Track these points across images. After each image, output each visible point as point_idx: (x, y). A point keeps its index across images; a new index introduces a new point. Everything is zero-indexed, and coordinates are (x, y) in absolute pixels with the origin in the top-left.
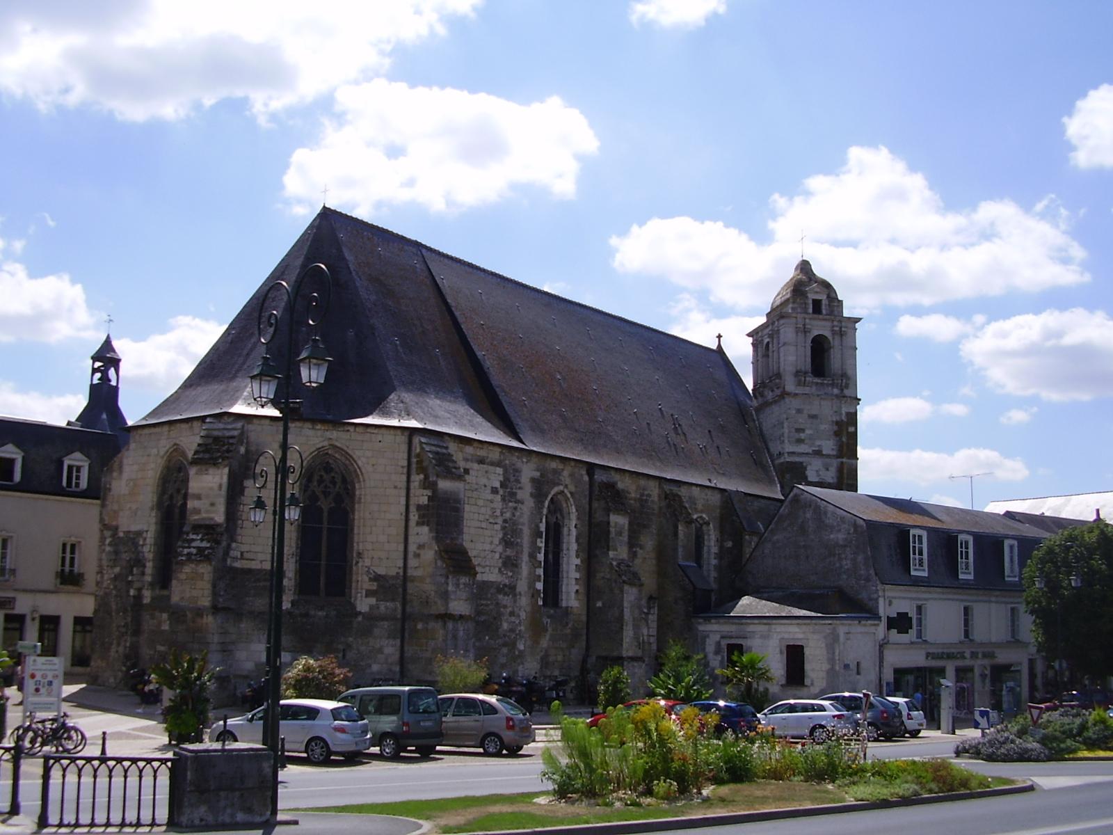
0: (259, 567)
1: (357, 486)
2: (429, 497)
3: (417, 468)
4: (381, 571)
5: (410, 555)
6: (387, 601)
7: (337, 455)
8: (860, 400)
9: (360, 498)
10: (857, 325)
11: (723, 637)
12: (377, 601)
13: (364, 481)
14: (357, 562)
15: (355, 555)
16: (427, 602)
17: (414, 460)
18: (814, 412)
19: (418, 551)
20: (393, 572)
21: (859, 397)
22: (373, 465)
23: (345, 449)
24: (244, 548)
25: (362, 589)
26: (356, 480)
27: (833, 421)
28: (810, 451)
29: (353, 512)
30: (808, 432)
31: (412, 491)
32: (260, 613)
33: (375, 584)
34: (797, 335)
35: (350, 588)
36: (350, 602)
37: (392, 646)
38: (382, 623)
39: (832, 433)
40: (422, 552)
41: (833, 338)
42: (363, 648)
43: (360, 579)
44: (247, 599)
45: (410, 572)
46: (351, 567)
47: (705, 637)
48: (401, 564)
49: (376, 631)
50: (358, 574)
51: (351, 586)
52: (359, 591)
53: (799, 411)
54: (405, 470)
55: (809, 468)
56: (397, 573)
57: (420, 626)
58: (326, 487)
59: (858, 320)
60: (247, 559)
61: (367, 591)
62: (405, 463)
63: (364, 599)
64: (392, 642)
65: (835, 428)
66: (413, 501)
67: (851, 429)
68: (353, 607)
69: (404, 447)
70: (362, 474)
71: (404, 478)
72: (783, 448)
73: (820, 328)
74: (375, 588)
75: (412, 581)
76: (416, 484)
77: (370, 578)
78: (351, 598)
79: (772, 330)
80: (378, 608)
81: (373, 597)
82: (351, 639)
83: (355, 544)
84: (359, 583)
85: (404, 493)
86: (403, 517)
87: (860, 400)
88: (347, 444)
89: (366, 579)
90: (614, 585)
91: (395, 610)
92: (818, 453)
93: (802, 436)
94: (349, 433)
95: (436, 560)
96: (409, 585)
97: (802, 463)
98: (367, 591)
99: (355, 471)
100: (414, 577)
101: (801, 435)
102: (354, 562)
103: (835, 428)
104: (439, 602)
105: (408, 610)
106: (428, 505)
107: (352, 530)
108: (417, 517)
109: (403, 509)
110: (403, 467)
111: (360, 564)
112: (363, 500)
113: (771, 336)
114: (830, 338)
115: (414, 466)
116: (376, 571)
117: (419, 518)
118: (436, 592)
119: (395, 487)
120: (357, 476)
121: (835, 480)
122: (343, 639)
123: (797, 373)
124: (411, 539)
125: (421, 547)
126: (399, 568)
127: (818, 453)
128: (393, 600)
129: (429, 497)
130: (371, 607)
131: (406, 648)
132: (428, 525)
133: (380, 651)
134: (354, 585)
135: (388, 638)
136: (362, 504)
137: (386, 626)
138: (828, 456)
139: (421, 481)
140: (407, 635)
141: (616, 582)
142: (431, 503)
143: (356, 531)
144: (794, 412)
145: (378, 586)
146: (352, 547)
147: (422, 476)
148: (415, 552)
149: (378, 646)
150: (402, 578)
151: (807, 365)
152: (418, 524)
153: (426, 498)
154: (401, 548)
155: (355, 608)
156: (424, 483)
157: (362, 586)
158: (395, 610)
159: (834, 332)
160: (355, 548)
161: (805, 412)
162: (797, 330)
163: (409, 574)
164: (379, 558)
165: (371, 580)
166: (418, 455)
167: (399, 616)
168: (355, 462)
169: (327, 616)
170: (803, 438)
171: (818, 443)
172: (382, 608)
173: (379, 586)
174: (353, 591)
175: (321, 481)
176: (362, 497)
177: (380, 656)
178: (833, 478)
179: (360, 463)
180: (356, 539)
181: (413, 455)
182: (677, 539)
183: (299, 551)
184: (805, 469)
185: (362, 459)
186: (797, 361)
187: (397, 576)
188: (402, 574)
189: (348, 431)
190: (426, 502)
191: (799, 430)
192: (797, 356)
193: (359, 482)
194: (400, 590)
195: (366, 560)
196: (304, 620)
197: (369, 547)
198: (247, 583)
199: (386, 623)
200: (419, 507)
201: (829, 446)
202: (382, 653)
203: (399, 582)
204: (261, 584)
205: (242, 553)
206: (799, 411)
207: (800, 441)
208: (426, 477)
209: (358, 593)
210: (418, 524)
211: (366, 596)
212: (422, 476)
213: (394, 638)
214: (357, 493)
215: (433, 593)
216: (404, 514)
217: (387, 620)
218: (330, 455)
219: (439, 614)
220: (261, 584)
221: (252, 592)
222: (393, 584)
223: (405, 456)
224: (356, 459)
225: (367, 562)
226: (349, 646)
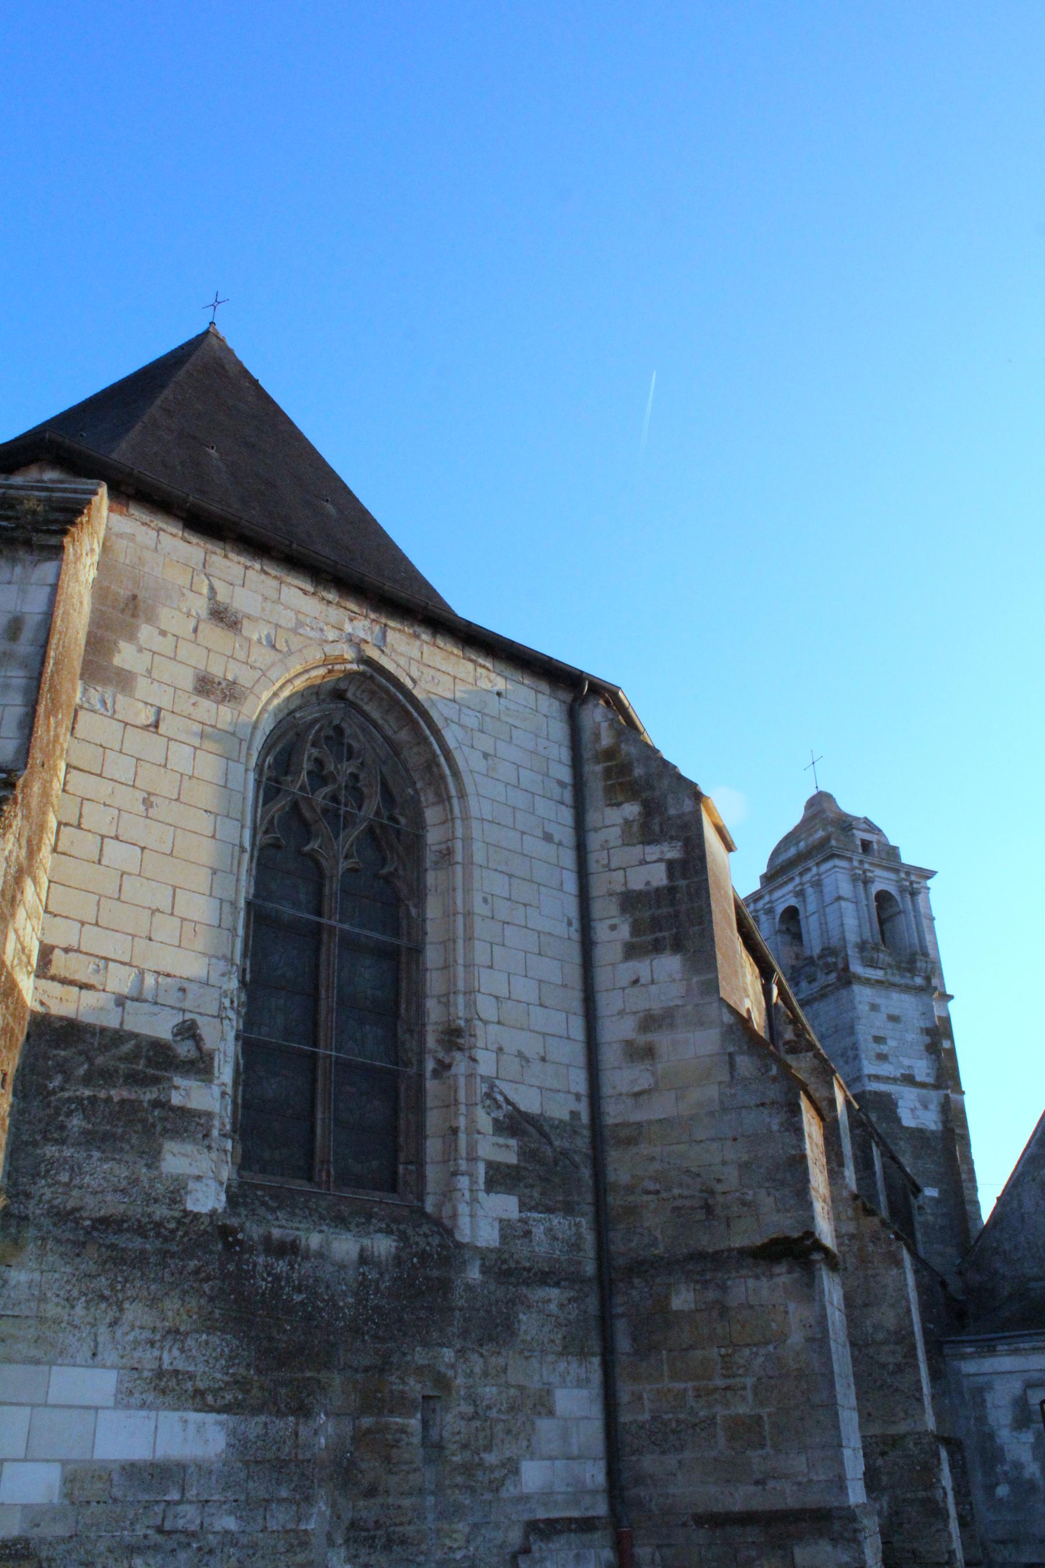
0: (112, 1021)
1: (431, 815)
2: (671, 865)
3: (609, 790)
4: (529, 1102)
5: (611, 1056)
6: (549, 1210)
7: (367, 708)
8: (951, 997)
9: (447, 855)
10: (930, 883)
11: (1029, 1385)
12: (523, 1206)
13: (462, 795)
14: (443, 1067)
15: (431, 1042)
16: (708, 1209)
17: (594, 770)
18: (896, 1012)
19: (642, 1039)
20: (559, 1109)
21: (949, 992)
22: (486, 756)
23: (409, 684)
24: (63, 934)
25: (472, 1159)
26: (427, 797)
27: (922, 1029)
28: (898, 1075)
29: (420, 895)
30: (891, 1043)
31: (596, 858)
32: (104, 1222)
33: (513, 1142)
34: (854, 887)
35: (419, 1161)
36: (425, 1215)
37: (580, 1383)
38: (540, 1293)
39: (923, 1048)
40: (662, 1040)
41: (902, 898)
42: (489, 1391)
43: (462, 1122)
44: (51, 1151)
45: (614, 1113)
46: (421, 1090)
47: (980, 1393)
48: (579, 1082)
49: (528, 1324)
50: (450, 1104)
51: (420, 1150)
52: (463, 1165)
53: (874, 1007)
54: (568, 795)
55: (900, 1103)
56: (574, 1115)
57: (682, 1300)
58: (334, 799)
59: (929, 874)
60: (64, 981)
61: (490, 1165)
62: (565, 774)
63: (482, 1195)
64: (574, 1368)
65: (928, 1040)
66: (599, 886)
67: (946, 1044)
68: (445, 1230)
69: (559, 729)
70: (456, 773)
71: (567, 816)
72: (860, 1070)
73: (883, 881)
74: (512, 1159)
75: (630, 1142)
76: (613, 835)
77: (496, 1121)
78: (421, 1197)
79: (801, 884)
80: (528, 1233)
81: (509, 1192)
82: (448, 1354)
83: (431, 1004)
84: (462, 1137)
85: (569, 858)
86: (576, 936)
87: (951, 997)
88: (415, 674)
89: (484, 1121)
90: (871, 1248)
91: (576, 1246)
92: (909, 1080)
93: (884, 1049)
94: (418, 643)
95: (731, 1055)
96: (613, 1155)
97: (888, 1095)
98: (490, 1165)
99: (432, 763)
100: (639, 1125)
101: (882, 1047)
102: (430, 1065)
103: (928, 1040)
104: (767, 1202)
105: (618, 1244)
106: (672, 890)
107: (417, 950)
108: (624, 932)
109: (572, 909)
110: (561, 784)
111: (460, 1066)
112: (459, 857)
113: (800, 894)
114: (898, 898)
115: (596, 786)
116: (513, 1097)
117: (636, 930)
118: (744, 1167)
119: (548, 838)
120: (437, 781)
121: (940, 1127)
122: (420, 1356)
123: (862, 947)
124: (608, 1003)
125: (649, 1022)
126: (578, 1097)
127: (909, 1080)
128: (569, 1209)
129: (671, 865)
130: (506, 1227)
131: (624, 1395)
132: (677, 946)
133: (544, 1405)
134: (433, 1147)
135: (565, 1352)
136: (459, 868)
137: (553, 1307)
138: (923, 1085)
139: (628, 823)
140: (624, 1344)
141: (875, 1239)
142: (682, 883)
143: (432, 956)
144: (867, 1008)
145: (522, 1153)
146: (421, 1011)
147: (632, 810)
148: (629, 1043)
149: (534, 1384)
150: (586, 1133)
151: (871, 931)
152: (631, 951)
153: (662, 867)
154: (577, 1028)
155: (450, 1232)
156: (645, 826)
157: (472, 1147)
158: (576, 1246)
159: (902, 890)
160: (434, 1011)
161: (883, 1009)
162: (854, 879)
163: (610, 1121)
164: (520, 1055)
165: (499, 1127)
166: (610, 754)
167: (590, 1269)
168: (437, 732)
169: (363, 1259)
170: (885, 1052)
171: (906, 1062)
172: (538, 1232)
173: (527, 1154)
174: (432, 1173)
175: (319, 776)
176: (459, 845)
177: (544, 1425)
178: (936, 1122)
179: (452, 744)
180: (434, 983)
181: (587, 754)
182: (874, 1174)
183: (243, 997)
184: (896, 1105)
185: (454, 727)
186: (860, 926)
187: (570, 1127)
188: (585, 1118)
189: (417, 636)
190: (664, 882)
191: (879, 1040)
192: (859, 919)
193: (443, 798)
194: (586, 1173)
195: (480, 1055)
196: (281, 1266)
197: (486, 1007)
198: (57, 1081)
199: (554, 1293)
200: (630, 901)
201: (922, 1069)
202: (551, 1413)
203: (582, 1143)
204: (117, 1094)
205: (46, 953)
206: (874, 1007)
207: (882, 1057)
208: (651, 809)
209: (455, 1174)
210: (631, 951)
211: (491, 1186)
212: (632, 810)
213: (583, 1354)
214: (433, 837)
215: (731, 1175)
216: (576, 924)
217: (557, 1284)
218: (352, 704)
219: (774, 1242)
220: (117, 1094)
221: (76, 1122)
222: (564, 1153)
223: (565, 755)
224: (440, 723)
225: (486, 1065)
226: (443, 1383)
